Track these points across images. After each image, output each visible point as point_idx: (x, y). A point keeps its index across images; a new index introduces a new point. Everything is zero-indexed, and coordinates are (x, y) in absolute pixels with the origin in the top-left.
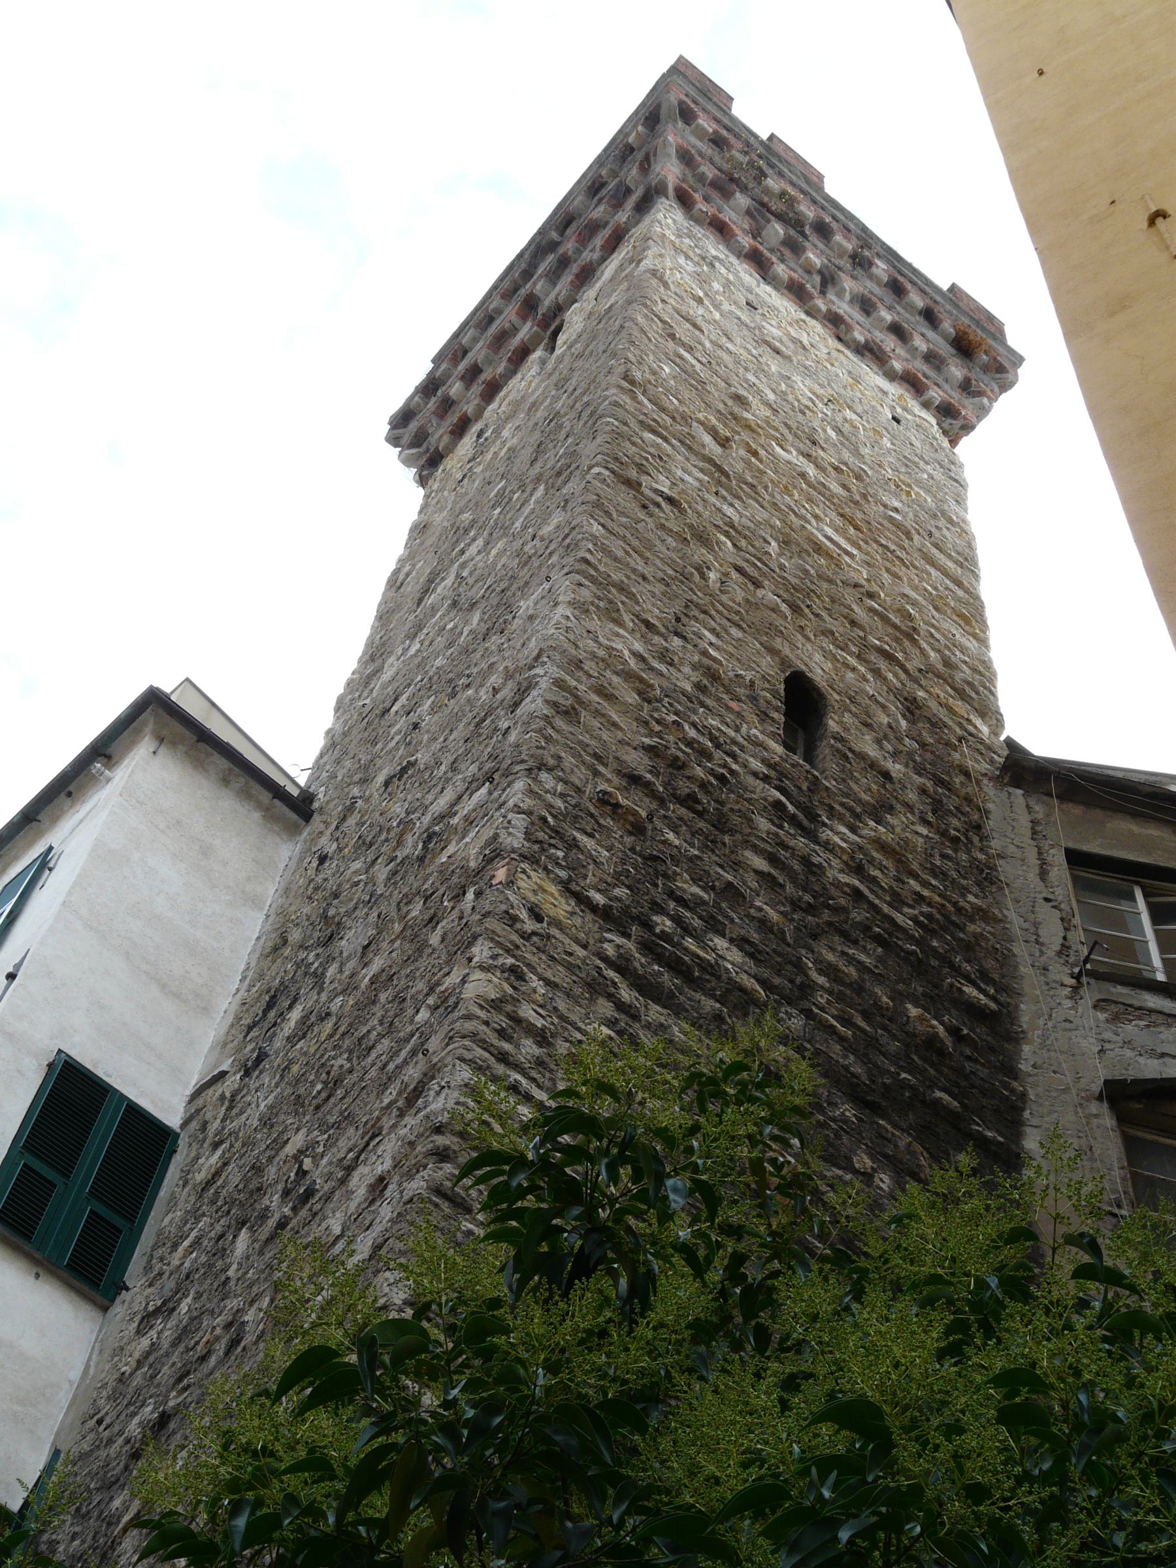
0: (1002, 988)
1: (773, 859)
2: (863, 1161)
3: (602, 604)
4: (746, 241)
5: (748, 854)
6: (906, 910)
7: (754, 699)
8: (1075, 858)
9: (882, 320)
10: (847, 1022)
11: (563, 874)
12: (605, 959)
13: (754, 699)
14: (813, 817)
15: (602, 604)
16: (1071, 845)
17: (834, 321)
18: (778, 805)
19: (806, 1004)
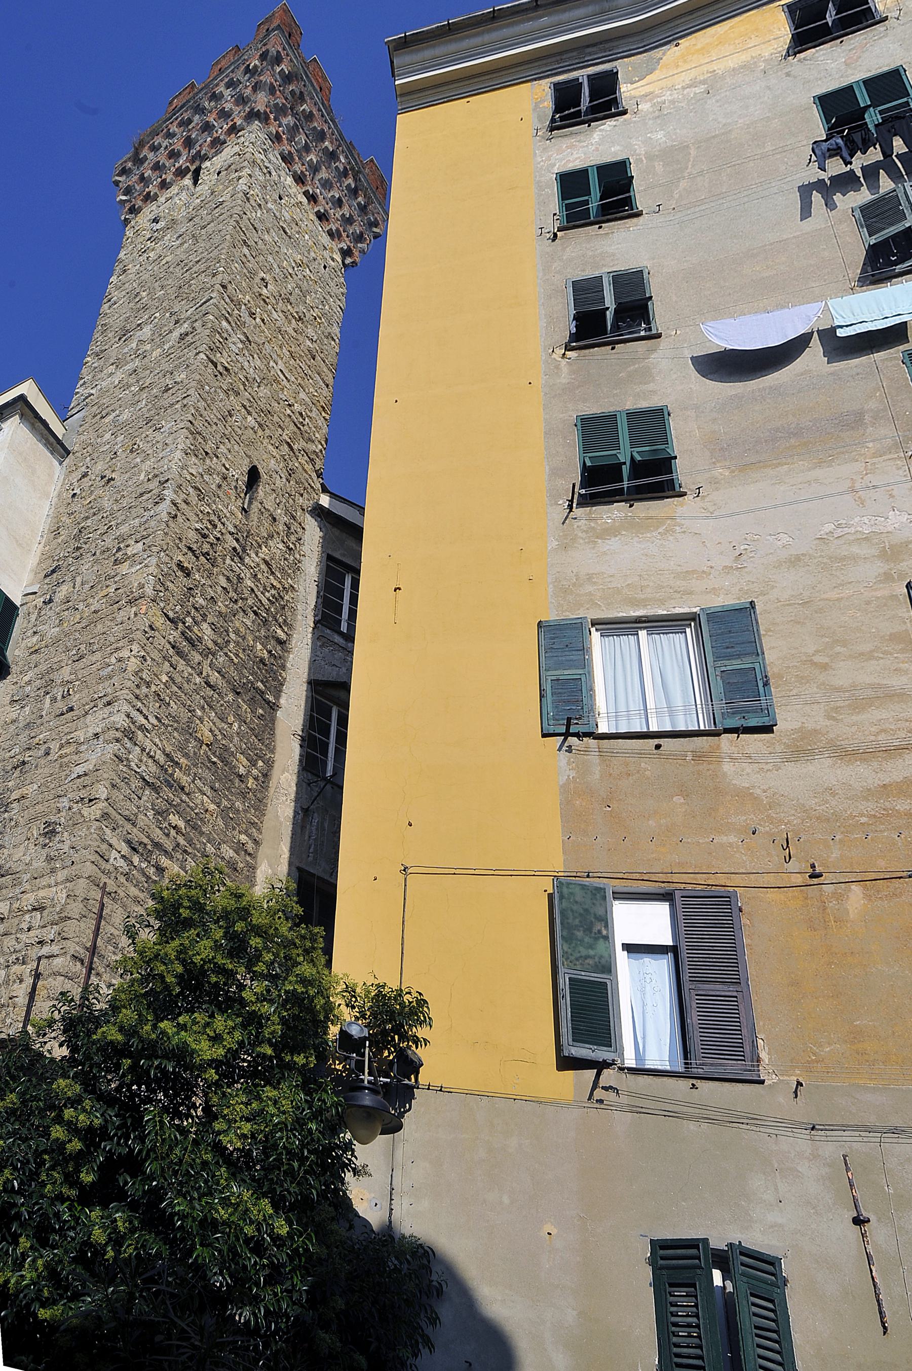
0: (290, 627)
1: (228, 579)
2: (231, 719)
3: (192, 447)
4: (286, 148)
5: (221, 577)
6: (267, 594)
7: (236, 487)
8: (330, 558)
9: (333, 196)
10: (237, 655)
11: (162, 605)
12: (170, 643)
13: (236, 487)
14: (244, 550)
15: (192, 447)
16: (330, 553)
17: (312, 198)
18: (234, 549)
19: (226, 650)
